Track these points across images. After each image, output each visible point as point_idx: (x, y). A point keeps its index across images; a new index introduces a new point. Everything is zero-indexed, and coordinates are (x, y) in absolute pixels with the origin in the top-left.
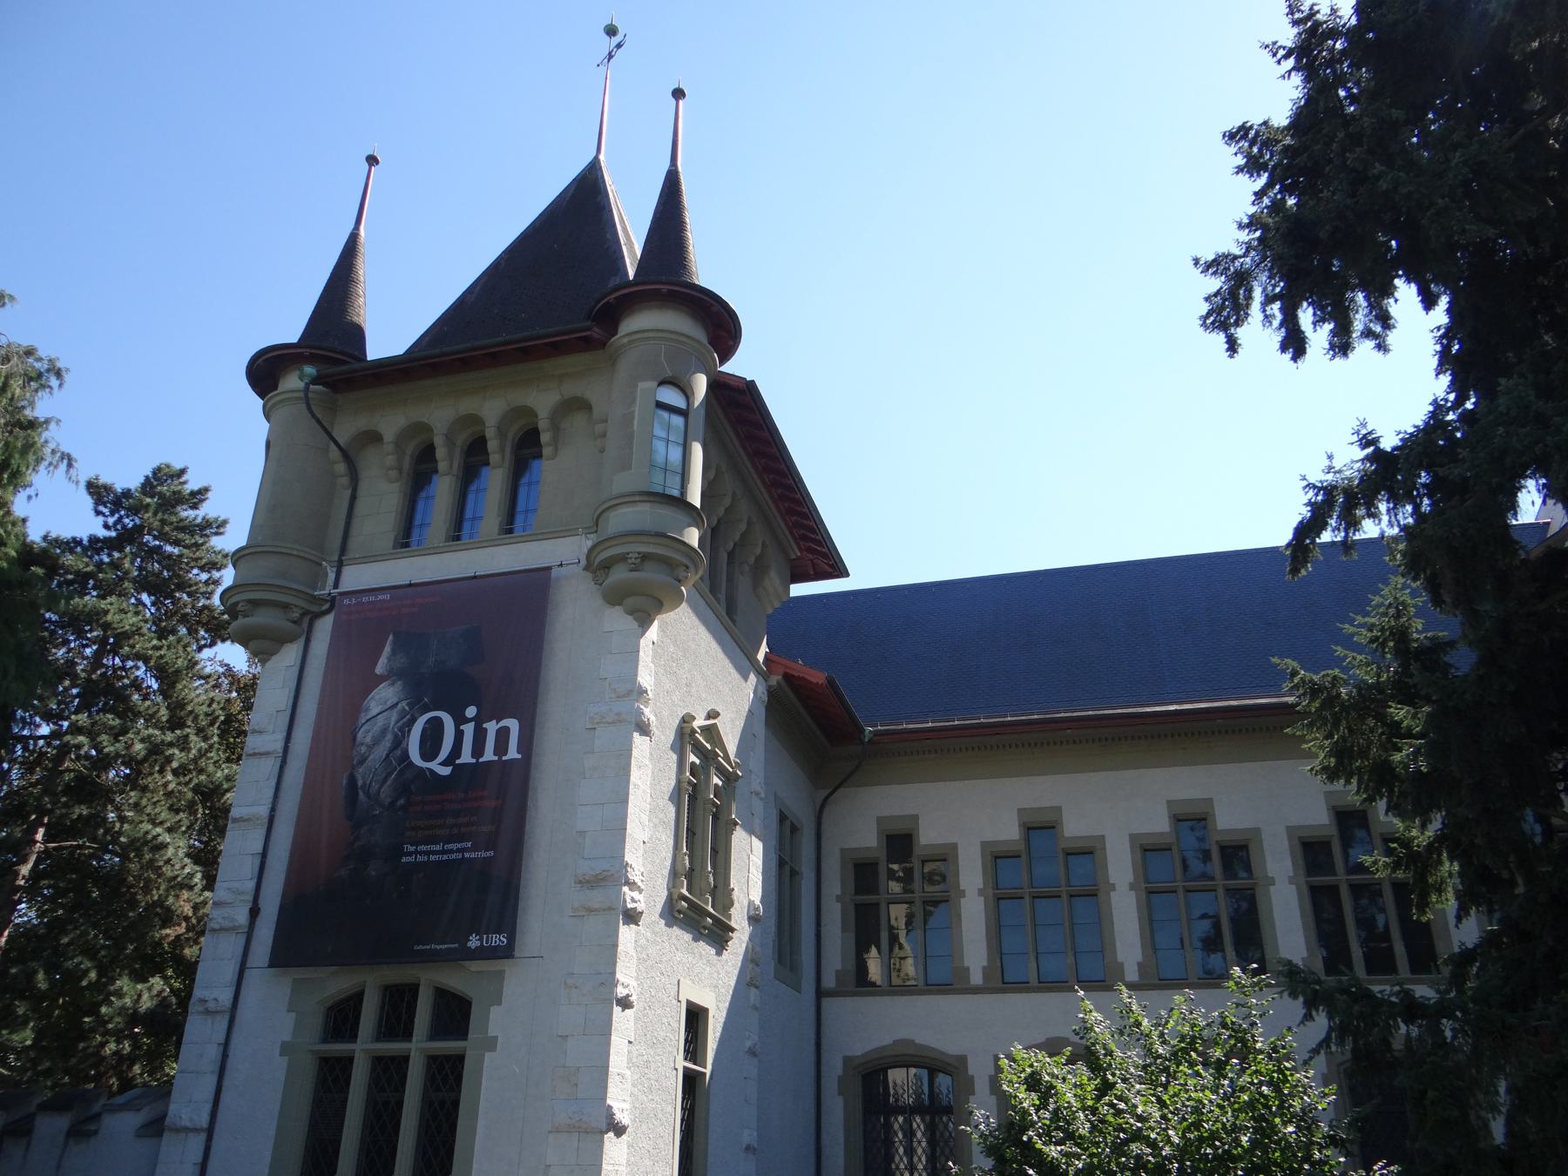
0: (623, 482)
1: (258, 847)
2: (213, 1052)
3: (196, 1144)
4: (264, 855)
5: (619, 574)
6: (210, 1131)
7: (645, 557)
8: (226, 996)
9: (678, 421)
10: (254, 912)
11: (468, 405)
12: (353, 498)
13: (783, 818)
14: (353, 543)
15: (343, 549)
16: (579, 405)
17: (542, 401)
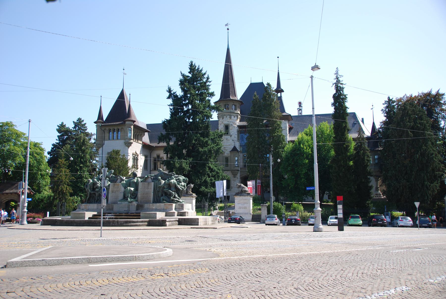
11: (114, 127)
17: (120, 128)
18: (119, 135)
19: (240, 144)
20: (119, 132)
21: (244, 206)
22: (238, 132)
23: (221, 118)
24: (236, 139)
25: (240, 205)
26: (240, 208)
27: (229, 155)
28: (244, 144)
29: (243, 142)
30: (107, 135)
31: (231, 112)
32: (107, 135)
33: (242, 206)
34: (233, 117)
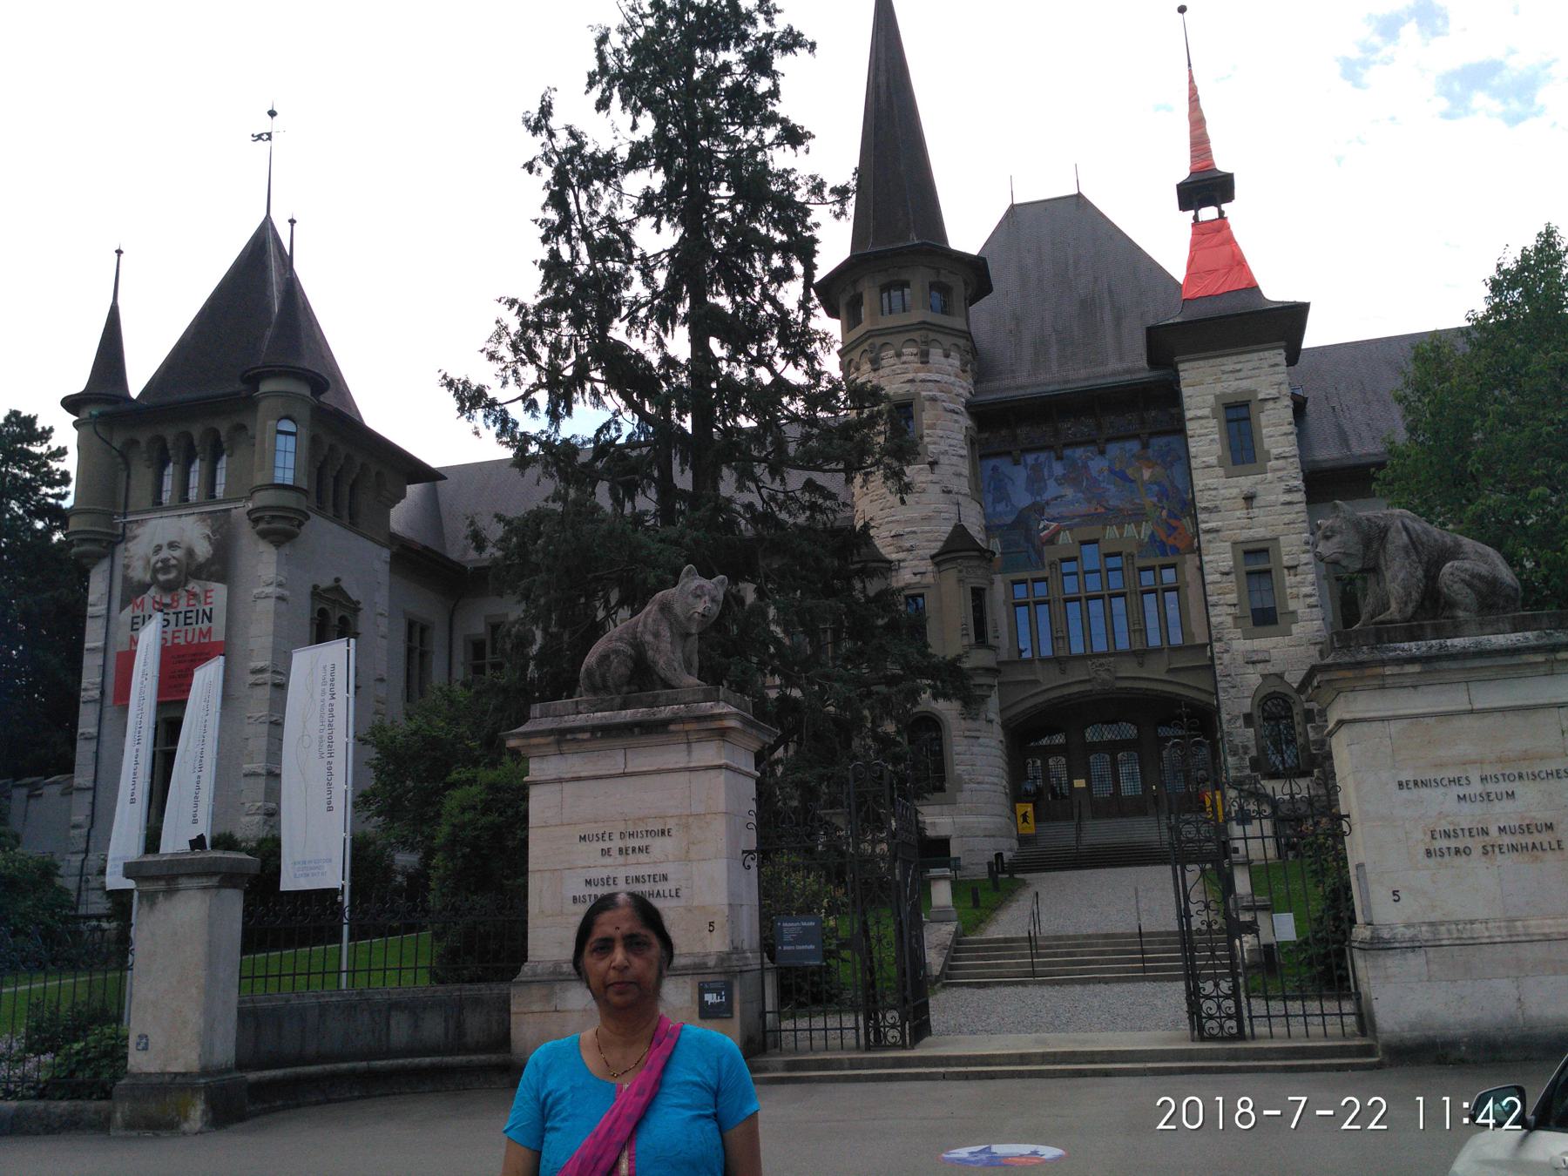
0: (259, 479)
1: (100, 662)
2: (91, 755)
3: (89, 796)
4: (104, 666)
5: (262, 526)
6: (94, 789)
7: (273, 517)
8: (93, 730)
9: (291, 439)
10: (102, 693)
12: (128, 476)
13: (411, 625)
14: (131, 501)
15: (126, 506)
16: (241, 428)
18: (221, 477)
19: (986, 516)
20: (223, 463)
21: (1504, 813)
22: (972, 442)
23: (866, 367)
24: (963, 486)
25: (1441, 805)
26: (1447, 845)
27: (929, 579)
28: (1009, 519)
29: (1000, 507)
30: (142, 475)
31: (923, 326)
32: (142, 475)
33: (1468, 815)
34: (936, 354)
